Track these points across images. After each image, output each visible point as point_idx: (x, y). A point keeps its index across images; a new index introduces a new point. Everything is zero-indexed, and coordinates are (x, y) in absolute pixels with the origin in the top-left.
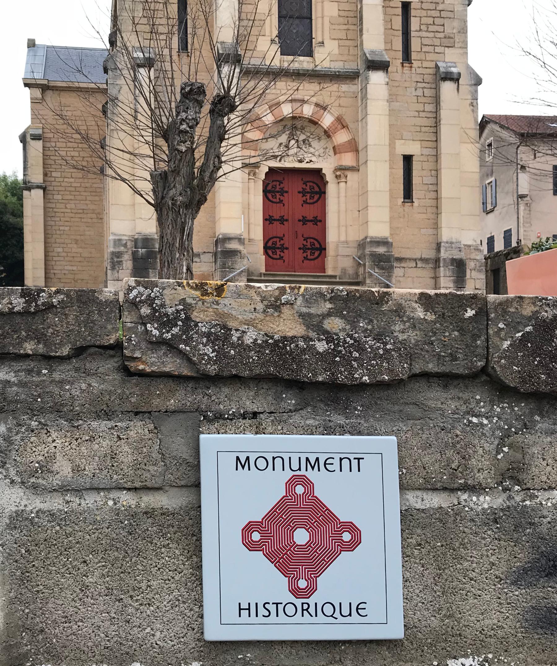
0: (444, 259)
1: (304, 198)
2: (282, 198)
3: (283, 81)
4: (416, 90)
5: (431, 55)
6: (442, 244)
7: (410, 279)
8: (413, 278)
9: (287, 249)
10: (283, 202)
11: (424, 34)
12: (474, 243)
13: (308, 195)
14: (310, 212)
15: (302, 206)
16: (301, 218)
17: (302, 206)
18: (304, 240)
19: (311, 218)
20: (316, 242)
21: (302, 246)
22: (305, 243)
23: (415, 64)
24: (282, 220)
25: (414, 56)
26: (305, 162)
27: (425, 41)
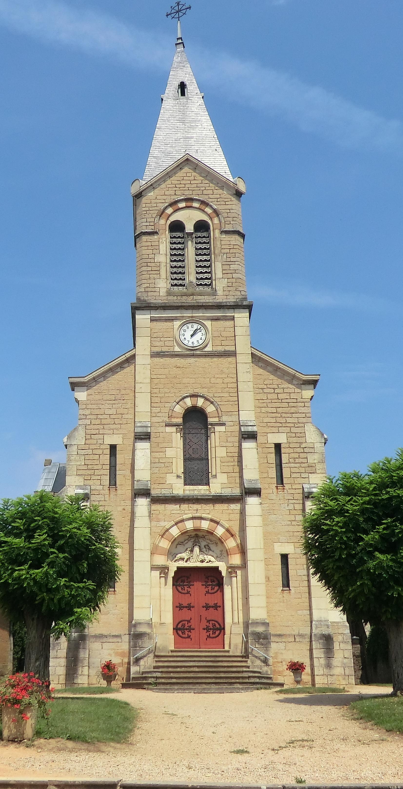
23: (287, 487)
24: (189, 607)
26: (206, 562)
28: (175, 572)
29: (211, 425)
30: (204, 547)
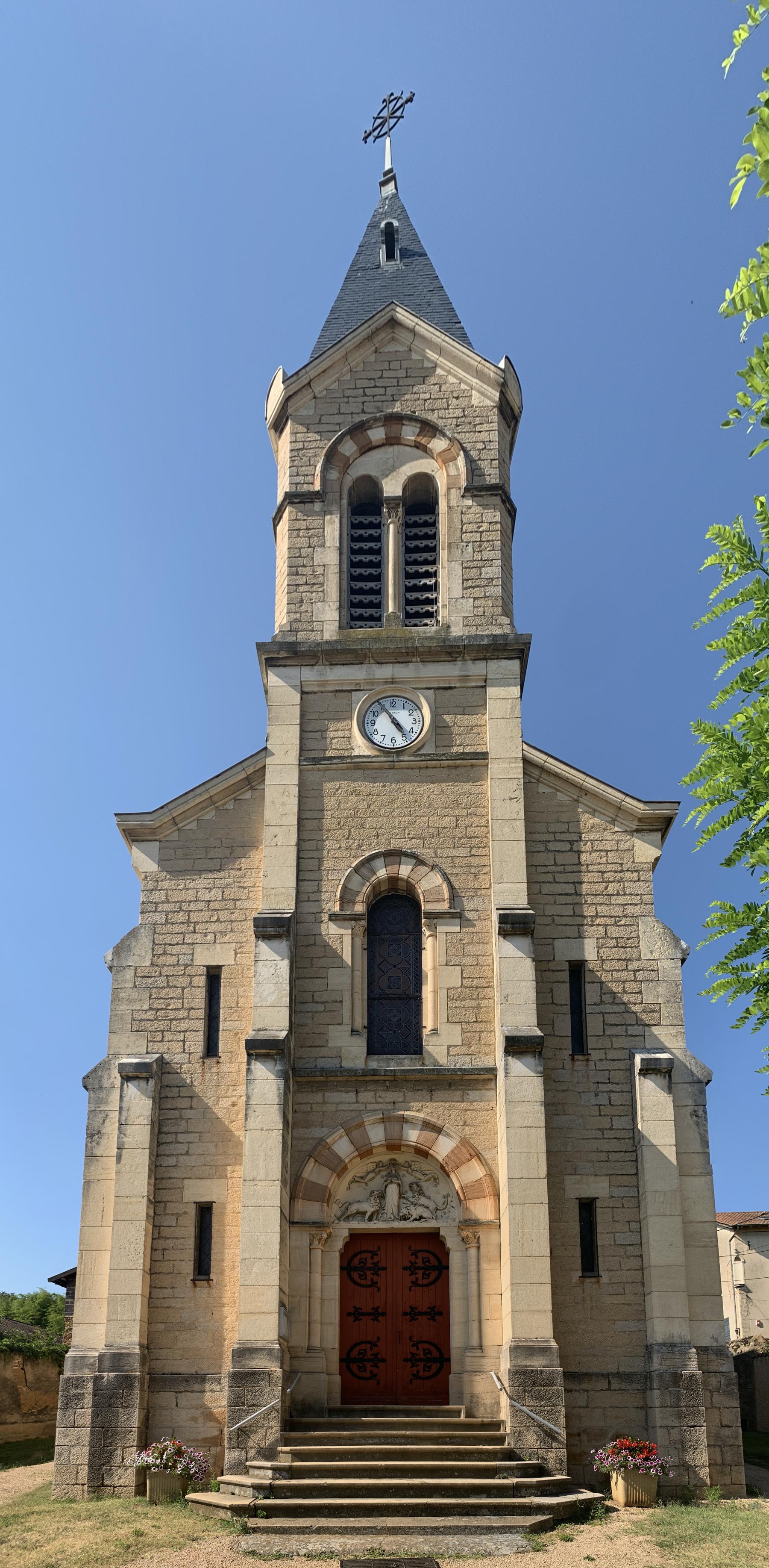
0: (661, 1376)
1: (413, 1278)
2: (375, 1278)
3: (370, 1090)
4: (596, 1095)
5: (620, 1039)
6: (656, 1348)
7: (599, 1410)
8: (604, 1408)
9: (384, 1360)
10: (378, 1285)
11: (608, 1008)
12: (715, 1344)
13: (420, 1272)
14: (423, 1299)
15: (410, 1290)
16: (408, 1310)
17: (410, 1290)
18: (413, 1346)
19: (425, 1309)
20: (433, 1349)
21: (409, 1356)
22: (414, 1350)
23: (595, 1055)
25: (591, 1043)
26: (412, 1219)
27: (611, 1019)
28: (347, 1245)
29: (431, 916)
30: (408, 1190)
